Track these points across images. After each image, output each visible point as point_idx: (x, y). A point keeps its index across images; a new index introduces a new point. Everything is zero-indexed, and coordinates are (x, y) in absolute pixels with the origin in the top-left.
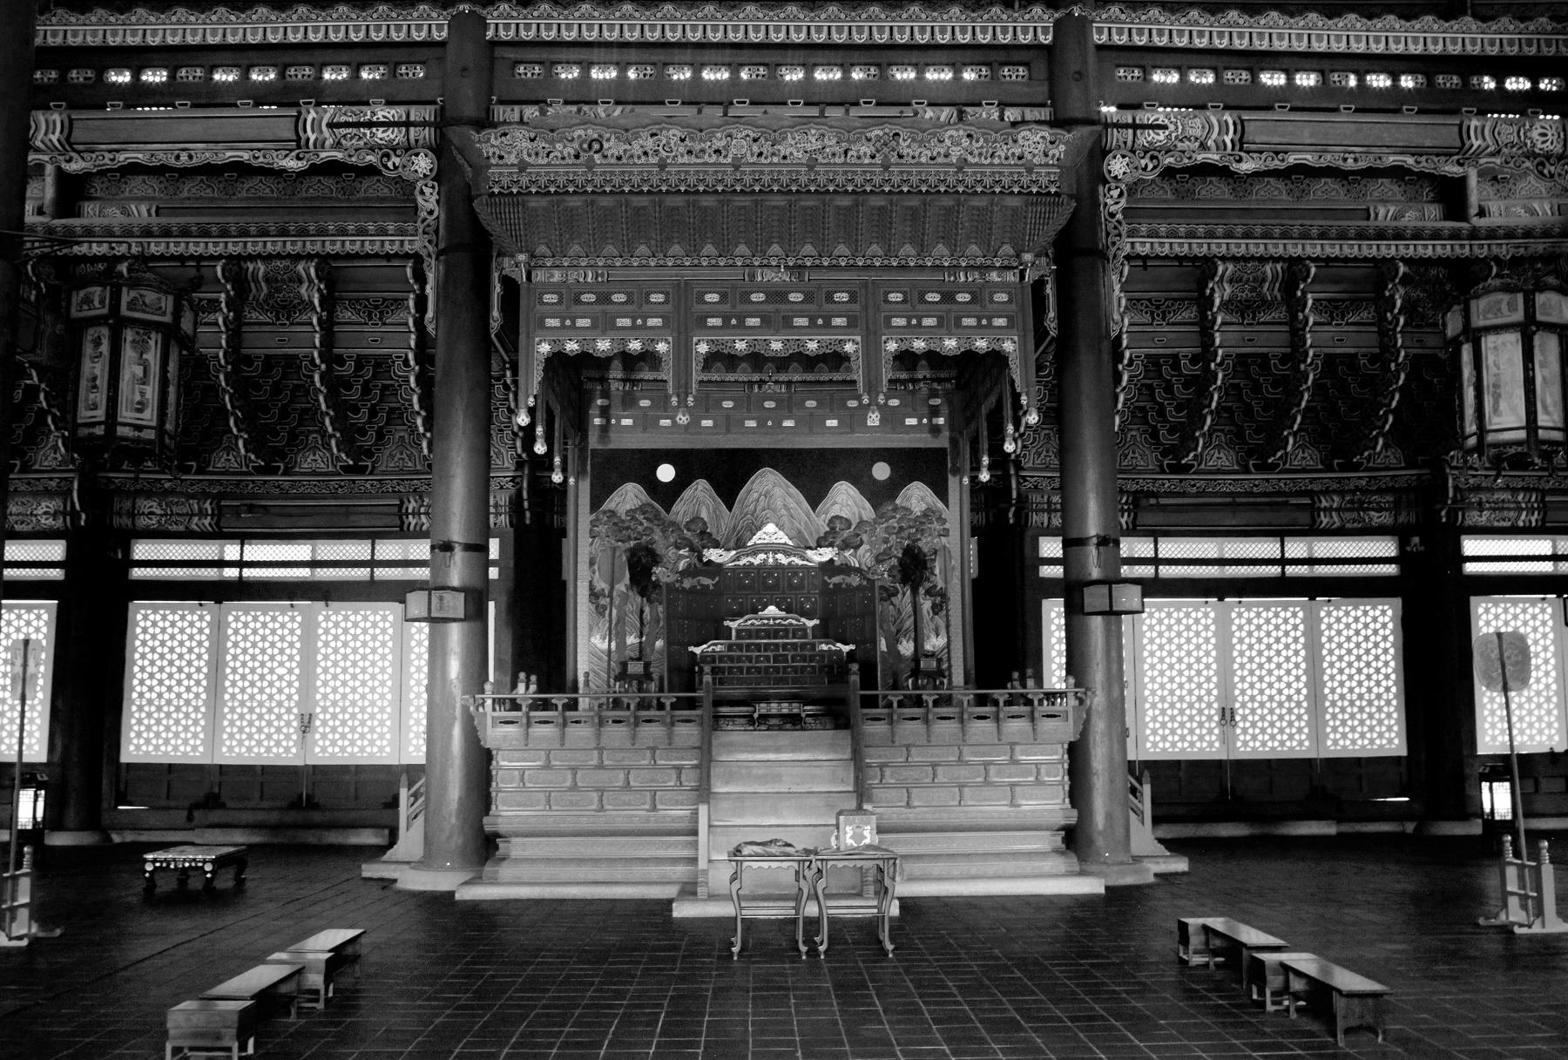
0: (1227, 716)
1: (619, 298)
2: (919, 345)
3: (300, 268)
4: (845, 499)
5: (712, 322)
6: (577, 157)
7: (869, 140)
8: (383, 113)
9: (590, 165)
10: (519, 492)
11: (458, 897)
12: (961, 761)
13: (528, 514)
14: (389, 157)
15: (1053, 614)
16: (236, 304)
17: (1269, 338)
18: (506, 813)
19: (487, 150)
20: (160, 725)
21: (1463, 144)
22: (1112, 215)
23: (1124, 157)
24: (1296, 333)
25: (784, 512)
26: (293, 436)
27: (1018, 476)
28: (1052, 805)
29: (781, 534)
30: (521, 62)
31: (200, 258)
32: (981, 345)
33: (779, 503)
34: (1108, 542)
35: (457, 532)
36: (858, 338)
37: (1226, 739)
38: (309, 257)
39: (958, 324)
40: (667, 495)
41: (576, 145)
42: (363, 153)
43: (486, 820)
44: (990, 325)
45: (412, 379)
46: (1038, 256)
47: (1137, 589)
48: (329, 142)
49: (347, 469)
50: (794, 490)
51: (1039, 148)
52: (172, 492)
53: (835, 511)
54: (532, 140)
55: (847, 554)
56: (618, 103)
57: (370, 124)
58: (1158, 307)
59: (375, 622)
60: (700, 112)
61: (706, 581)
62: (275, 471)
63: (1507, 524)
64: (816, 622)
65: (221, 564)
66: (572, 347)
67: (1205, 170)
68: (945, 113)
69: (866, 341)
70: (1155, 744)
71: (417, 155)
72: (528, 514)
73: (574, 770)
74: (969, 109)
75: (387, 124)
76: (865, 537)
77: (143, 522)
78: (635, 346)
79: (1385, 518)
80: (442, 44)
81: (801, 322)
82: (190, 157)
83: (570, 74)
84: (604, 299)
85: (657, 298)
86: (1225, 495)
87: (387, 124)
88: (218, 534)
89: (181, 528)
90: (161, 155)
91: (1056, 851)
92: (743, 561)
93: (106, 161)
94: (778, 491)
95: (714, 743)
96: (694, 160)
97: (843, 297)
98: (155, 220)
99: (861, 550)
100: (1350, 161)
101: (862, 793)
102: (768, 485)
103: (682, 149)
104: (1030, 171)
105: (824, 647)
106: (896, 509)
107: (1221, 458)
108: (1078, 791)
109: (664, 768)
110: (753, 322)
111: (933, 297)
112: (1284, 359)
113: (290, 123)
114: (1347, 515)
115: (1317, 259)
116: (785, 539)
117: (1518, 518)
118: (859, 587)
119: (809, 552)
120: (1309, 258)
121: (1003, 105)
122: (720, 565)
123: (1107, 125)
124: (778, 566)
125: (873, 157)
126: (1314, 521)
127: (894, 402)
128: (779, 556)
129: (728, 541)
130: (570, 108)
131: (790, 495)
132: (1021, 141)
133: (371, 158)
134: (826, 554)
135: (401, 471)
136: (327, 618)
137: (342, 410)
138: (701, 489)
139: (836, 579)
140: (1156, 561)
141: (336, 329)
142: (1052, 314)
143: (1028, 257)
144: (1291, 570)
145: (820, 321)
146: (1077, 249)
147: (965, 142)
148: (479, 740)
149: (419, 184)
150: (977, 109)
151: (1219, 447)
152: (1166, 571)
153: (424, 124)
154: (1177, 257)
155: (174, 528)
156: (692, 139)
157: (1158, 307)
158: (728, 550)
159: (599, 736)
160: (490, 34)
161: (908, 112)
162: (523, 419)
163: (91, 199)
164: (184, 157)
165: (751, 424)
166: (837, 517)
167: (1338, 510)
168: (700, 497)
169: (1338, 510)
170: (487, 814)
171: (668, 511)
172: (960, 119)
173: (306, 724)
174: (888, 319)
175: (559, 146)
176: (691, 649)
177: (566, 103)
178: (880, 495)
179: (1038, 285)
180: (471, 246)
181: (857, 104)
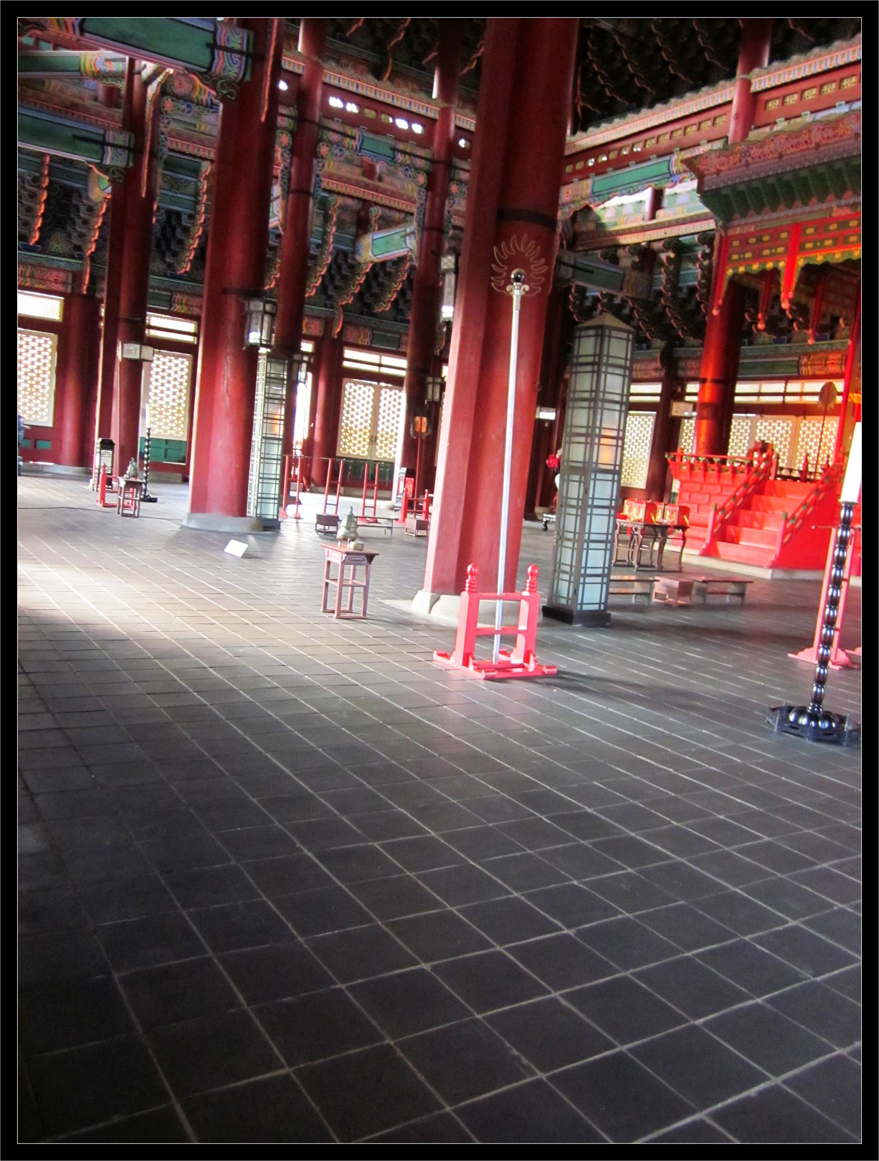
1: (766, 238)
6: (740, 161)
9: (747, 164)
30: (806, 90)
80: (730, 102)
96: (795, 150)
103: (788, 145)
110: (829, 242)
113: (666, 164)
136: (761, 424)
155: (645, 377)
175: (731, 158)
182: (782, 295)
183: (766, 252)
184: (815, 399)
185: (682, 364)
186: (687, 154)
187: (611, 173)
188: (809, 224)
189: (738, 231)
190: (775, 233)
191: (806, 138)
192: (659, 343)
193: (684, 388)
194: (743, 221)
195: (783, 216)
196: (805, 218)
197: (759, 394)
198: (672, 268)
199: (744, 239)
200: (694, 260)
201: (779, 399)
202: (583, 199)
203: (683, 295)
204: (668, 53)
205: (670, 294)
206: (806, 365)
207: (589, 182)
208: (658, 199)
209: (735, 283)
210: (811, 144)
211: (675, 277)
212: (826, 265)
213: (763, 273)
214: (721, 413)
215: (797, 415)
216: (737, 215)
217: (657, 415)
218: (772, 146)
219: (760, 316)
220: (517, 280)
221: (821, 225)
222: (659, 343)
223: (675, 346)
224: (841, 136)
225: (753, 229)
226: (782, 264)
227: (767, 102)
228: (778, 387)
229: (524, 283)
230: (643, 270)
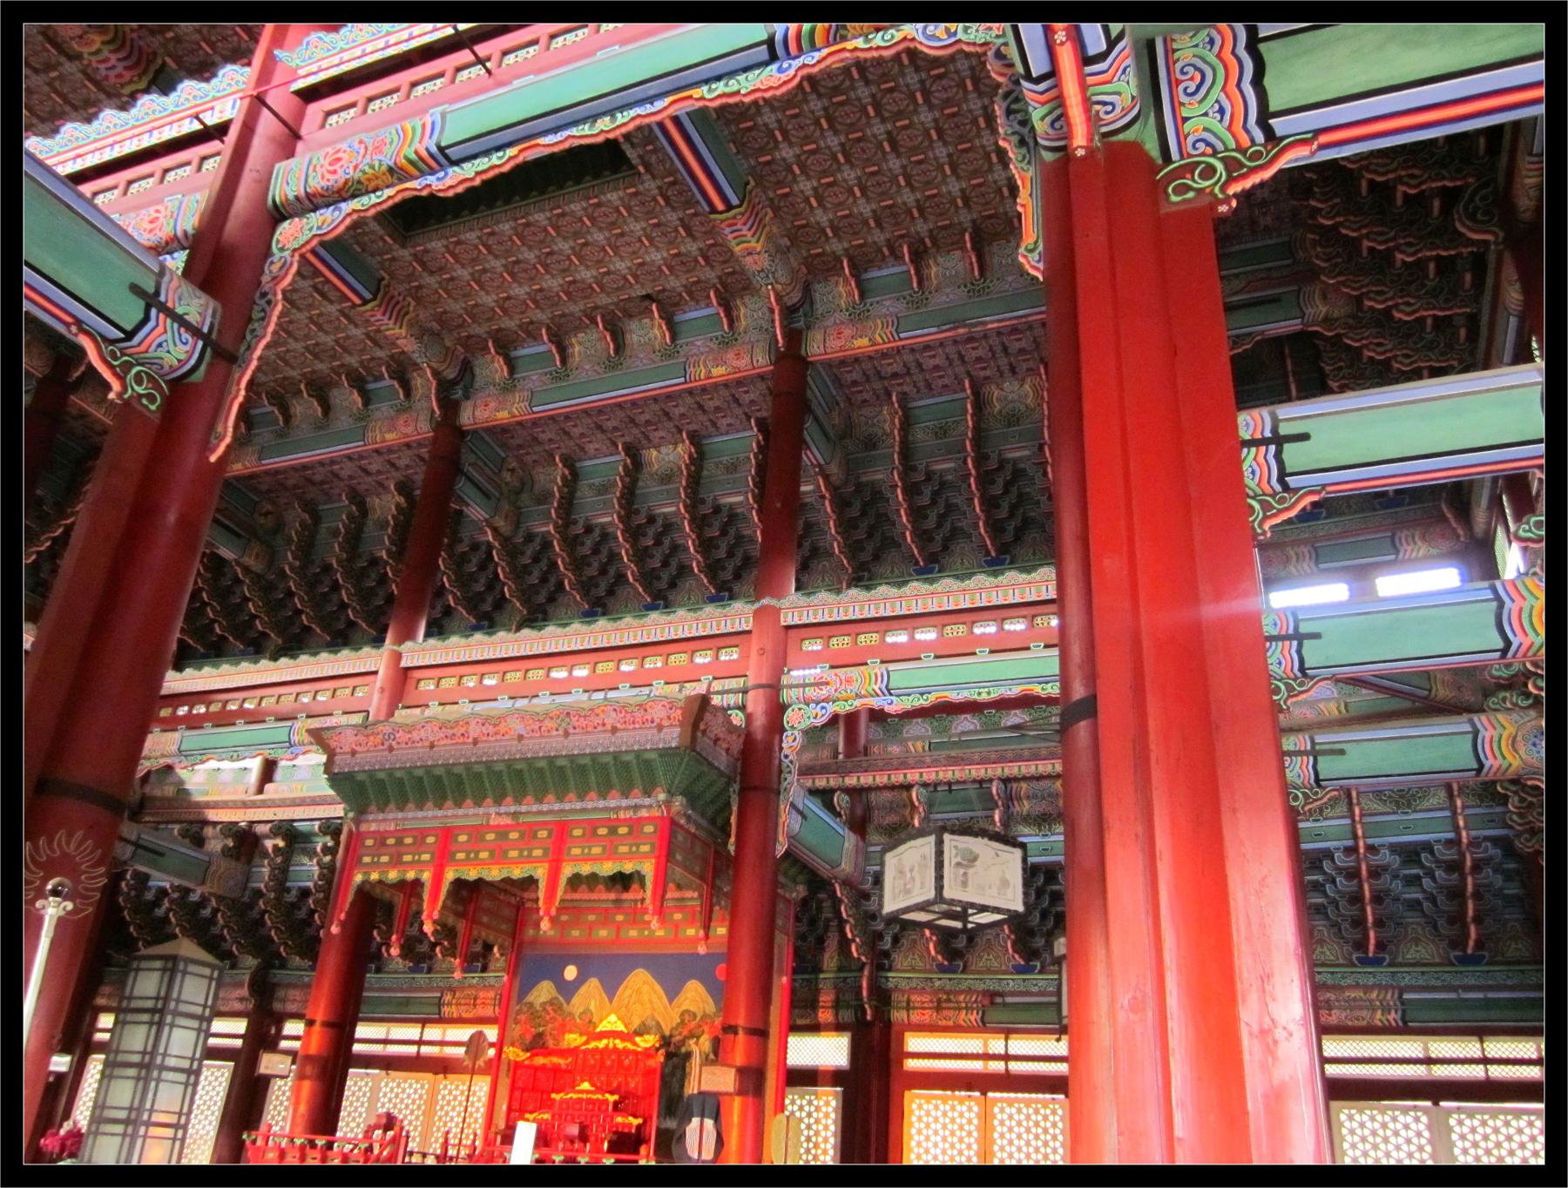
1: (408, 841)
9: (391, 749)
32: (628, 868)
33: (646, 998)
40: (568, 990)
50: (658, 987)
61: (561, 1061)
64: (616, 1097)
76: (706, 1028)
80: (375, 673)
81: (513, 854)
83: (471, 683)
94: (646, 988)
97: (543, 834)
99: (702, 1039)
105: (619, 1119)
111: (602, 831)
117: (1372, 1017)
119: (638, 1039)
124: (615, 1049)
138: (593, 984)
142: (732, 840)
147: (613, 714)
165: (633, 933)
166: (687, 1011)
182: (424, 917)
183: (407, 858)
184: (461, 1051)
185: (281, 993)
186: (316, 723)
187: (209, 728)
188: (462, 828)
189: (373, 827)
191: (462, 730)
192: (250, 962)
193: (280, 1030)
194: (381, 816)
195: (430, 816)
197: (386, 1042)
198: (279, 860)
199: (381, 838)
200: (312, 854)
201: (413, 1049)
202: (163, 756)
203: (291, 897)
204: (301, 600)
205: (272, 895)
206: (449, 1004)
207: (176, 735)
208: (269, 771)
211: (282, 874)
212: (480, 882)
213: (402, 885)
214: (330, 1071)
215: (436, 1073)
216: (373, 807)
219: (394, 937)
220: (55, 893)
221: (477, 832)
222: (250, 962)
223: (273, 967)
225: (392, 828)
226: (426, 876)
227: (419, 681)
228: (412, 1032)
229: (65, 899)
230: (238, 859)
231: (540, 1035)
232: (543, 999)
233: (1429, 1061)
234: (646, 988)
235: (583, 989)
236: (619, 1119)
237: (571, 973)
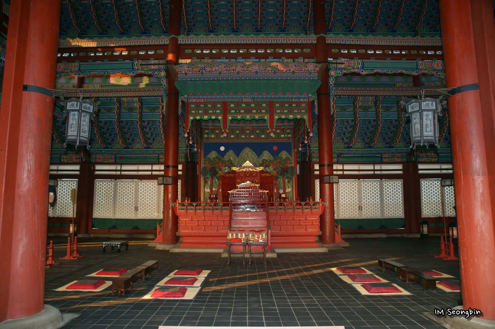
0: (360, 208)
2: (283, 117)
3: (134, 99)
4: (266, 155)
5: (233, 111)
6: (199, 71)
7: (271, 67)
8: (153, 62)
9: (202, 73)
10: (187, 153)
11: (170, 251)
12: (293, 219)
13: (189, 159)
14: (154, 72)
15: (317, 182)
16: (119, 108)
17: (371, 115)
18: (182, 231)
19: (177, 70)
20: (102, 210)
21: (418, 68)
22: (331, 85)
23: (334, 71)
24: (377, 114)
25: (251, 158)
26: (133, 140)
27: (309, 149)
28: (315, 230)
29: (250, 163)
31: (111, 97)
32: (299, 117)
33: (250, 156)
34: (330, 165)
35: (171, 163)
36: (268, 115)
37: (360, 214)
38: (137, 97)
39: (293, 112)
41: (199, 69)
42: (148, 71)
43: (177, 233)
44: (301, 112)
45: (161, 126)
46: (313, 95)
47: (337, 177)
48: (140, 69)
49: (146, 148)
50: (254, 153)
51: (312, 67)
52: (105, 153)
53: (264, 158)
54: (188, 68)
55: (267, 168)
56: (210, 58)
57: (150, 65)
58: (343, 108)
59: (152, 185)
60: (230, 60)
61: (232, 175)
62: (129, 148)
63: (429, 161)
64: (259, 185)
65: (116, 171)
66: (198, 118)
67: (354, 74)
68: (289, 60)
69: (270, 116)
70: (342, 215)
71: (161, 72)
72: (189, 159)
73: (198, 221)
74: (296, 59)
75: (155, 64)
76: (271, 164)
77: (98, 161)
78: (213, 117)
79: (400, 160)
80: (167, 45)
81: (254, 111)
82: (108, 73)
84: (206, 106)
85: (219, 106)
86: (360, 154)
87: (155, 64)
88: (115, 163)
89: (107, 162)
90: (101, 73)
91: (317, 242)
92: (241, 170)
93: (88, 74)
95: (233, 215)
96: (227, 72)
98: (100, 88)
100: (390, 72)
101: (268, 226)
102: (247, 151)
103: (225, 70)
104: (310, 74)
105: (261, 191)
106: (279, 157)
107: (359, 145)
108: (322, 226)
109: (220, 220)
110: (242, 111)
111: (287, 105)
112: (374, 121)
114: (389, 159)
115: (383, 96)
116: (251, 165)
118: (270, 177)
119: (257, 168)
120: (380, 96)
121: (304, 59)
122: (235, 171)
123: (330, 63)
124: (250, 171)
125: (272, 71)
126: (382, 160)
127: (278, 131)
128: (250, 169)
129: (237, 165)
130: (198, 60)
131: (253, 154)
132: (308, 67)
133: (150, 73)
134: (261, 168)
135: (159, 148)
136: (141, 184)
137: (145, 133)
139: (264, 175)
140: (343, 170)
141: (143, 114)
143: (310, 95)
144: (376, 172)
145: (259, 111)
146: (323, 92)
147: (294, 67)
148: (175, 213)
149: (162, 78)
150: (298, 59)
151: (359, 142)
152: (345, 173)
153: (163, 64)
154: (348, 96)
156: (227, 67)
157: (343, 108)
158: (237, 167)
159: (204, 212)
160: (179, 42)
161: (281, 60)
162: (186, 135)
163: (85, 83)
164: (106, 73)
165: (243, 136)
166: (264, 160)
167: (388, 158)
168: (230, 155)
169: (388, 158)
170: (177, 231)
171: (223, 158)
172: (294, 62)
173: (136, 209)
174: (276, 110)
176: (228, 191)
177: (197, 59)
178: (275, 154)
179: (313, 102)
180: (173, 93)
181: (268, 58)
189: (194, 101)
190: (214, 104)
191: (234, 68)
196: (229, 100)
201: (149, 173)
209: (197, 123)
210: (235, 71)
217: (79, 181)
218: (217, 68)
221: (238, 104)
224: (250, 71)
228: (149, 167)
231: (214, 167)
232: (213, 157)
233: (441, 169)
234: (249, 153)
235: (228, 153)
236: (261, 191)
237: (222, 149)
